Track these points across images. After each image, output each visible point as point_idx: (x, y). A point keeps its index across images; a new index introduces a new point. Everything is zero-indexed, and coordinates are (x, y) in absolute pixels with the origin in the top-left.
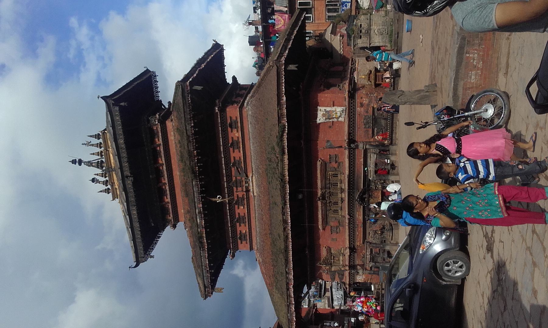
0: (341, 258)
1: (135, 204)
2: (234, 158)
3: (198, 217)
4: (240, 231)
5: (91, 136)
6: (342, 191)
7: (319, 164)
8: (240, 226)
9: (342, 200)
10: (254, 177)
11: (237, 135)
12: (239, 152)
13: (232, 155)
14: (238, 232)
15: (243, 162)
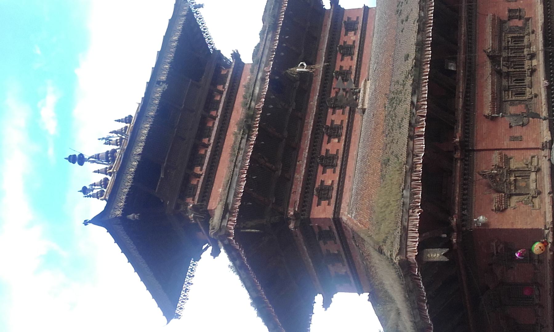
0: (533, 176)
1: (151, 120)
2: (341, 67)
3: (258, 83)
4: (322, 182)
5: (119, 121)
6: (533, 56)
7: (489, 19)
8: (324, 172)
9: (533, 71)
10: (369, 83)
11: (353, 38)
12: (352, 59)
13: (339, 63)
14: (318, 184)
15: (354, 72)
